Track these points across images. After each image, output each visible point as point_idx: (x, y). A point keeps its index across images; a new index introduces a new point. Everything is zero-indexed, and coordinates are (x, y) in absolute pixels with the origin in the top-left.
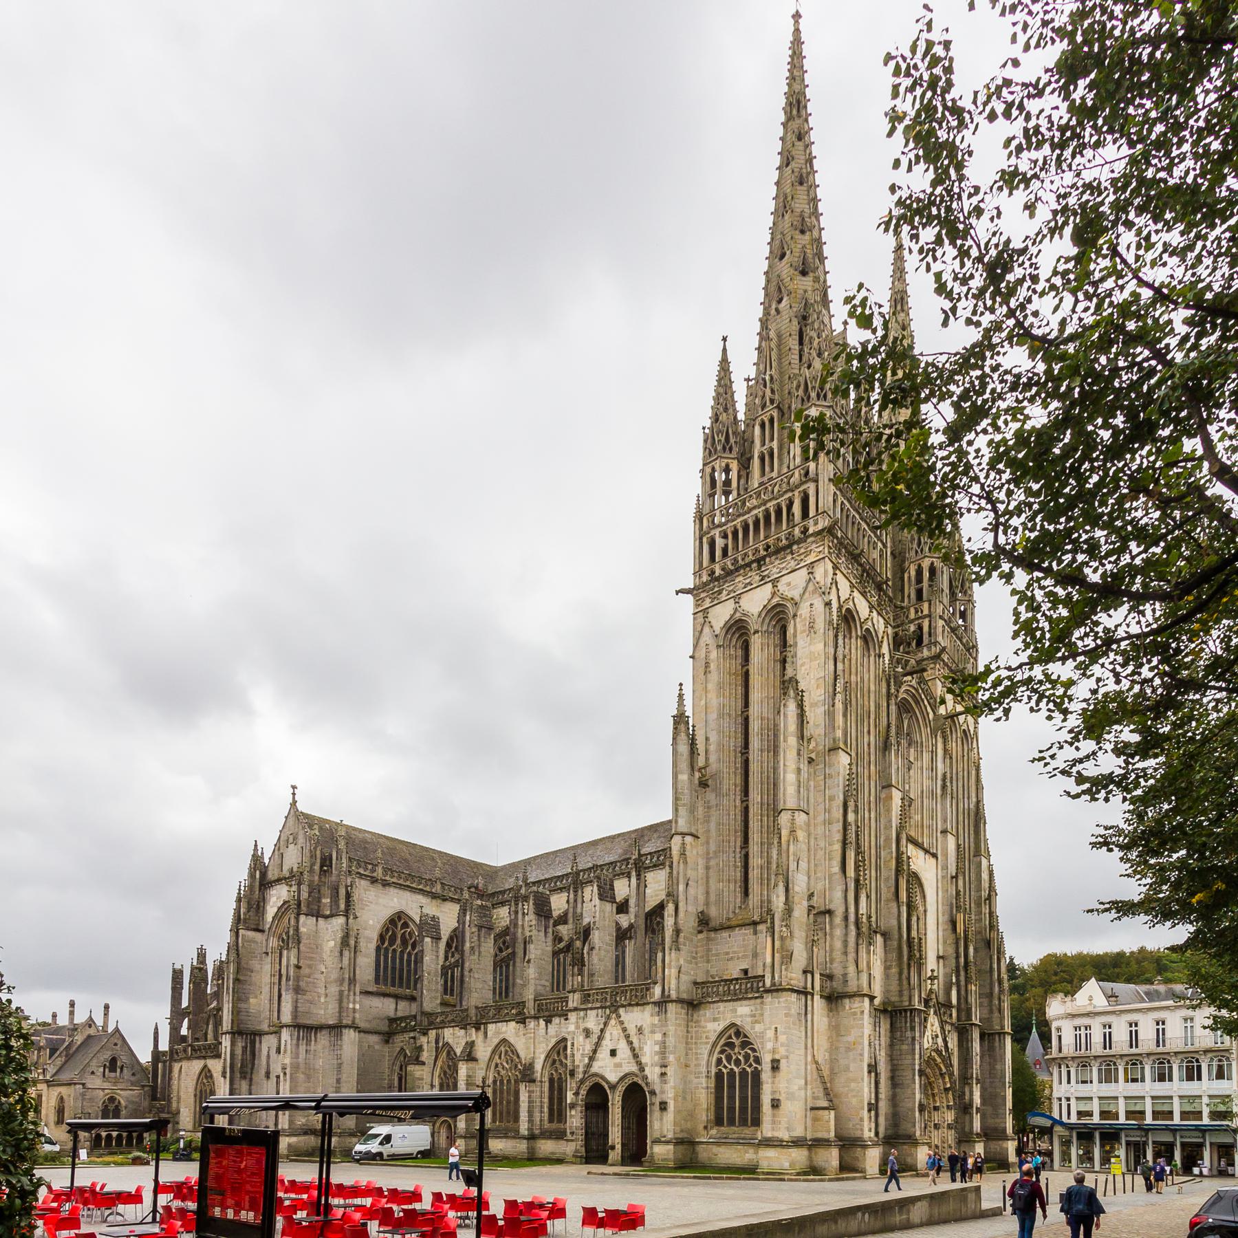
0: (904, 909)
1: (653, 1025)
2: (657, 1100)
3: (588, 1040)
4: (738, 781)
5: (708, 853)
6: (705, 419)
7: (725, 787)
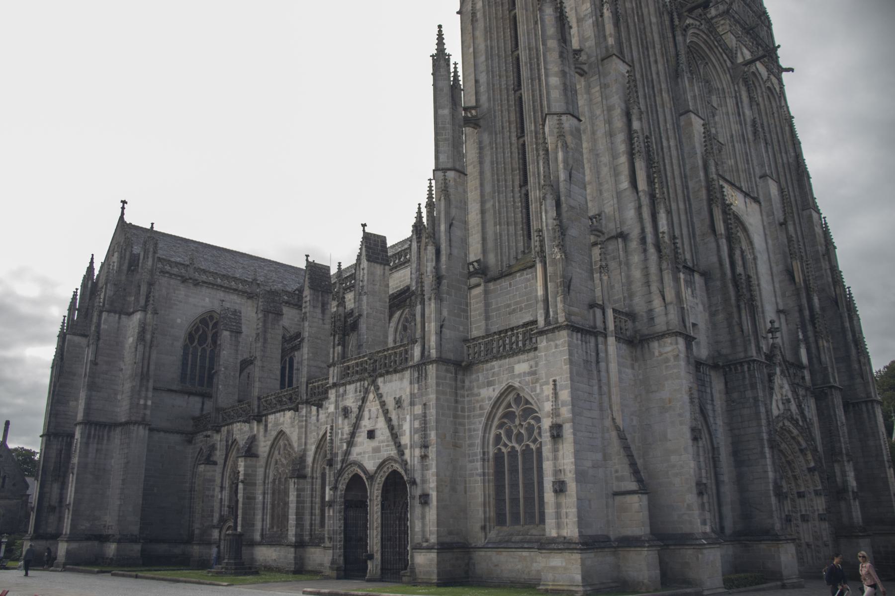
0: (723, 242)
1: (412, 395)
2: (418, 492)
3: (346, 421)
4: (513, 118)
5: (482, 195)
7: (498, 124)
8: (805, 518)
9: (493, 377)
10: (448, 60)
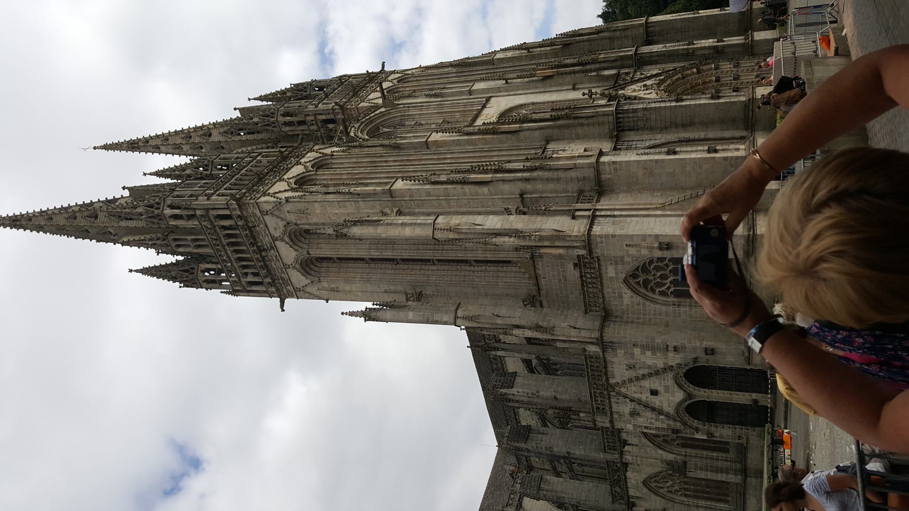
4: (418, 267)
6: (173, 287)
8: (736, 78)
9: (615, 294)
10: (370, 309)
